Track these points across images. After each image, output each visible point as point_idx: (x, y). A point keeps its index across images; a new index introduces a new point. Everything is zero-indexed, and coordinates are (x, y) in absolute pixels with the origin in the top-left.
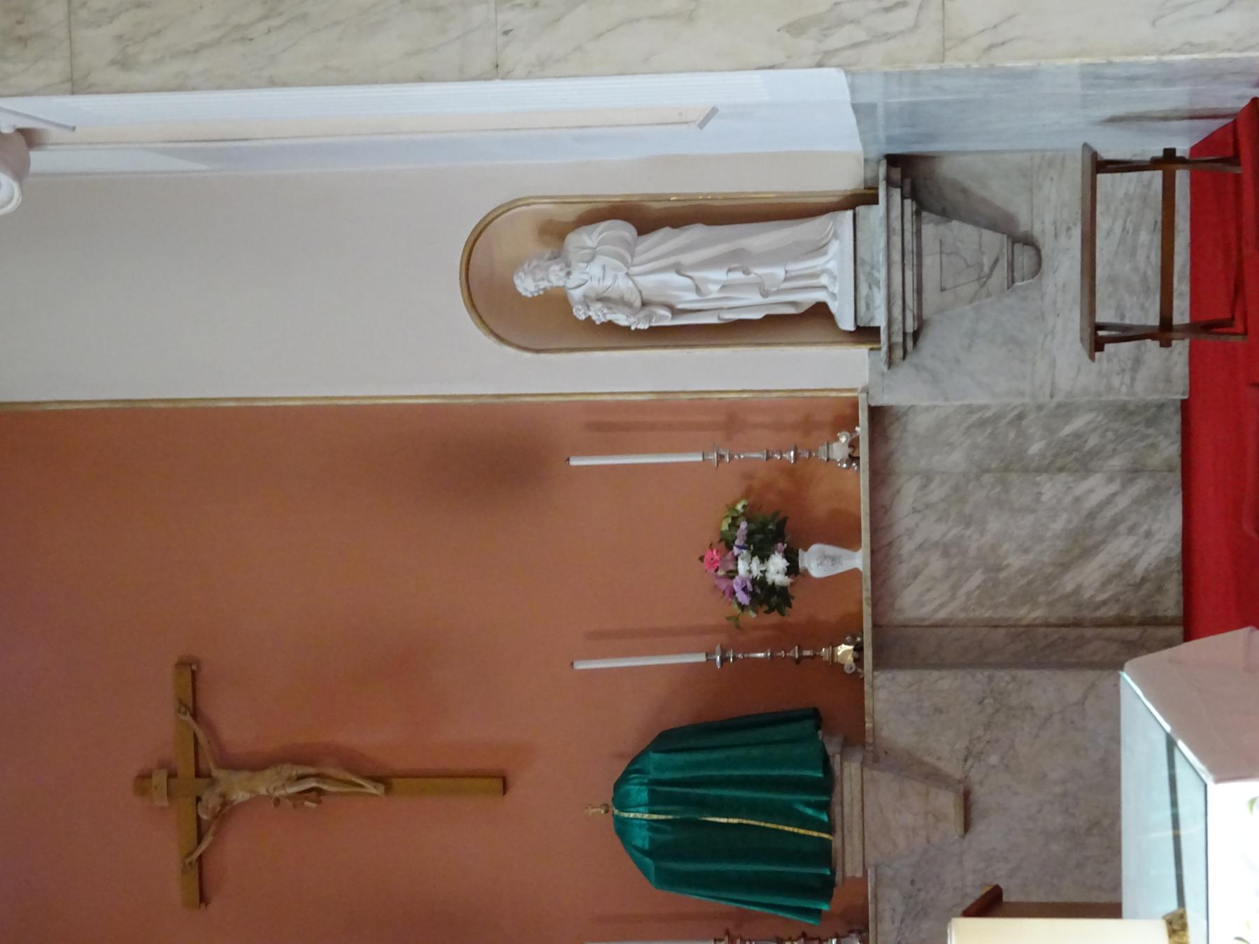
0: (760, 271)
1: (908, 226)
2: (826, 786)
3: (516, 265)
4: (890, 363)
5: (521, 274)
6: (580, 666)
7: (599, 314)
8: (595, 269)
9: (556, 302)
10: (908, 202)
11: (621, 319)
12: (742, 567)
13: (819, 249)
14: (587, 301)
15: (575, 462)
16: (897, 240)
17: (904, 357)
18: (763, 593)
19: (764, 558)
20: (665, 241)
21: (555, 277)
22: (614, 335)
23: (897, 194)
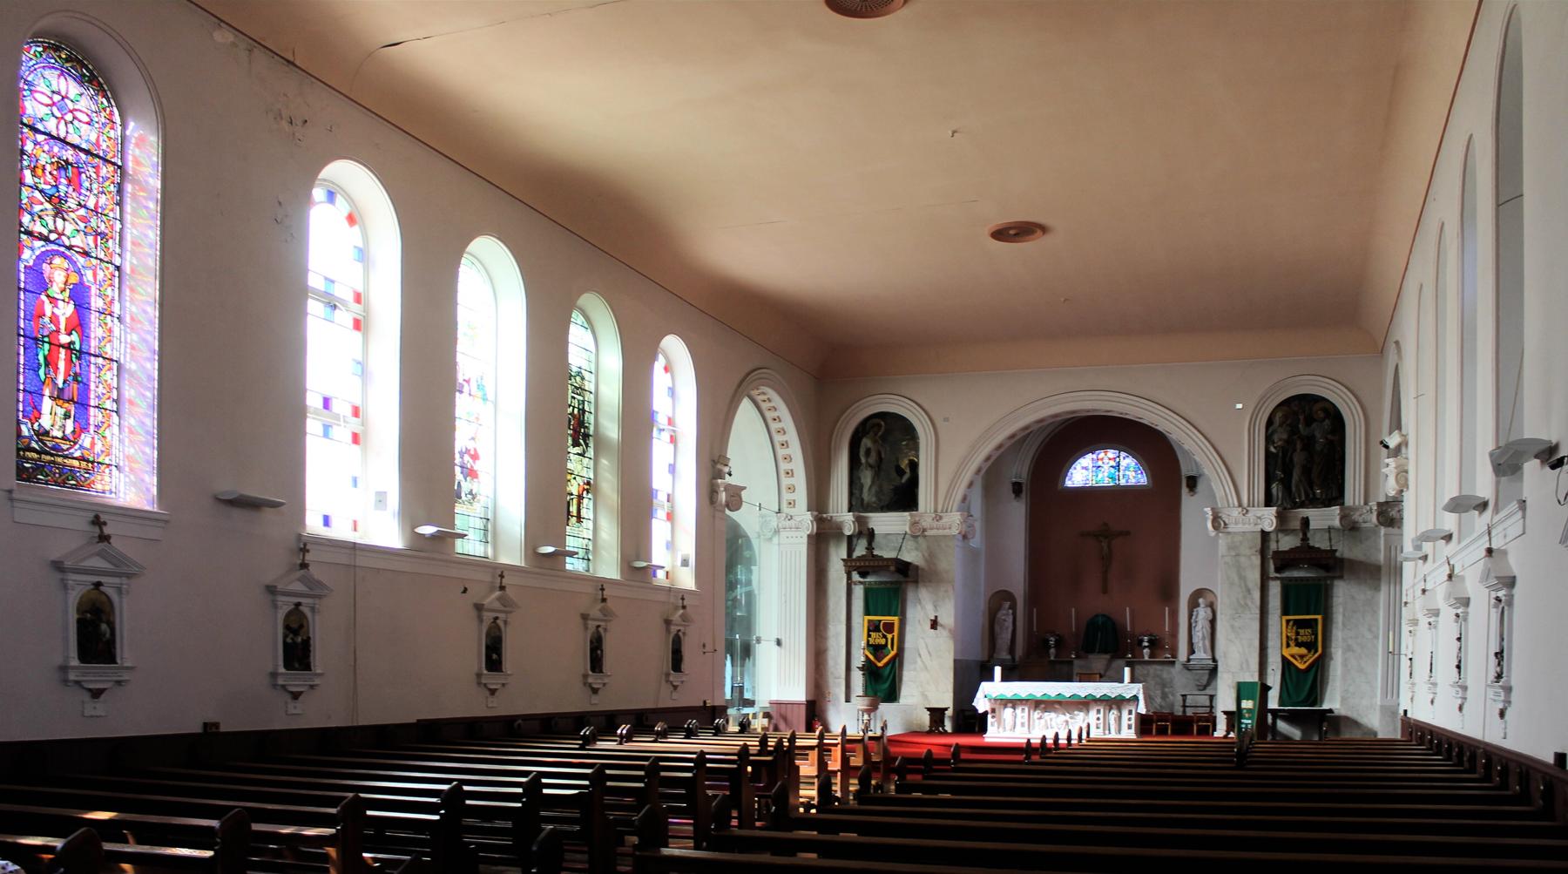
2: (1106, 652)
3: (1205, 598)
6: (1128, 609)
7: (1195, 613)
9: (1198, 605)
11: (1194, 617)
13: (1205, 652)
15: (1167, 609)
18: (1142, 641)
20: (1208, 626)
21: (1202, 605)
22: (1190, 616)
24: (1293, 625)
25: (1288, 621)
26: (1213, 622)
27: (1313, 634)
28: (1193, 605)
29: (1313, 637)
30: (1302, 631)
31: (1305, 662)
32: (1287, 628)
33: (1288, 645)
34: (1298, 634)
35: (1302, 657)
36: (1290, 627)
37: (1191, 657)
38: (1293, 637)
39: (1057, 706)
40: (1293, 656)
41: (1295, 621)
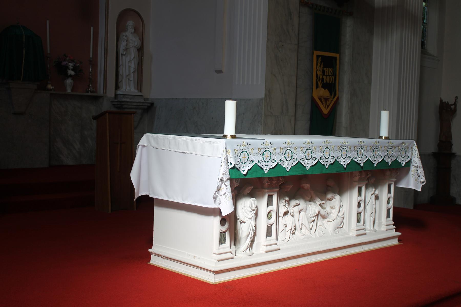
0: (132, 75)
1: (143, 107)
4: (112, 102)
5: (133, 23)
8: (134, 39)
9: (125, 30)
10: (147, 107)
12: (71, 64)
14: (126, 36)
16: (141, 104)
17: (114, 105)
18: (67, 68)
19: (72, 70)
23: (149, 105)
24: (321, 62)
25: (318, 57)
26: (140, 50)
27: (333, 75)
28: (120, 29)
29: (333, 77)
30: (326, 70)
31: (328, 106)
32: (317, 65)
33: (317, 87)
34: (324, 72)
35: (326, 99)
36: (319, 65)
37: (119, 92)
38: (321, 77)
39: (307, 186)
40: (320, 99)
41: (323, 57)
